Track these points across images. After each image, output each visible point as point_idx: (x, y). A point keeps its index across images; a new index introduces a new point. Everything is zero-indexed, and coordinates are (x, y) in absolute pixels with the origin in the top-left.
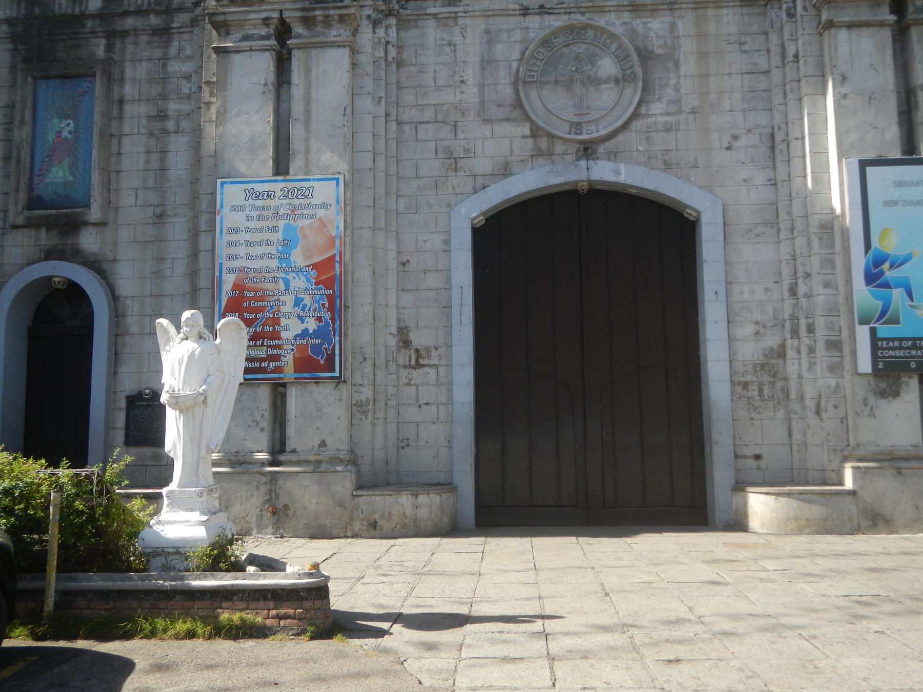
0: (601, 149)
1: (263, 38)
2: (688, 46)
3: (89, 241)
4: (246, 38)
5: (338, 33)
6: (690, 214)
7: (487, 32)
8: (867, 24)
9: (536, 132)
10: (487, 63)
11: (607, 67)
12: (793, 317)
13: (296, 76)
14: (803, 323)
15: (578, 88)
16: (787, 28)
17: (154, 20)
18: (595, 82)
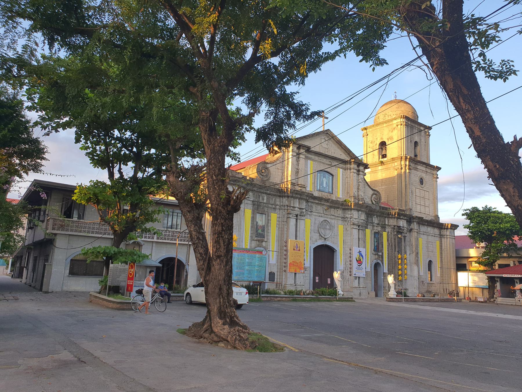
0: (327, 239)
1: (294, 216)
2: (336, 226)
3: (264, 244)
4: (292, 216)
5: (303, 218)
6: (335, 251)
7: (315, 218)
8: (356, 229)
9: (320, 235)
10: (315, 223)
11: (328, 227)
12: (345, 267)
13: (298, 224)
14: (347, 268)
15: (325, 230)
16: (347, 226)
17: (274, 206)
18: (326, 229)
